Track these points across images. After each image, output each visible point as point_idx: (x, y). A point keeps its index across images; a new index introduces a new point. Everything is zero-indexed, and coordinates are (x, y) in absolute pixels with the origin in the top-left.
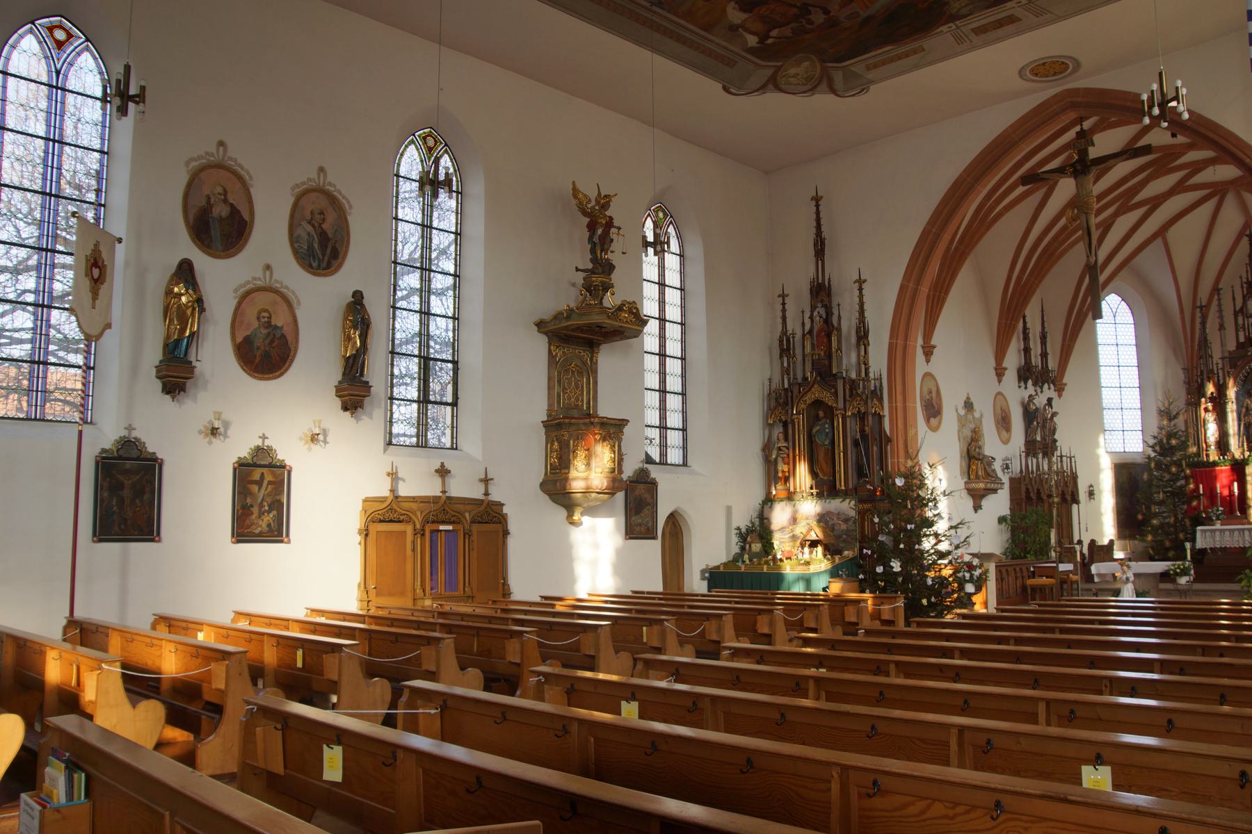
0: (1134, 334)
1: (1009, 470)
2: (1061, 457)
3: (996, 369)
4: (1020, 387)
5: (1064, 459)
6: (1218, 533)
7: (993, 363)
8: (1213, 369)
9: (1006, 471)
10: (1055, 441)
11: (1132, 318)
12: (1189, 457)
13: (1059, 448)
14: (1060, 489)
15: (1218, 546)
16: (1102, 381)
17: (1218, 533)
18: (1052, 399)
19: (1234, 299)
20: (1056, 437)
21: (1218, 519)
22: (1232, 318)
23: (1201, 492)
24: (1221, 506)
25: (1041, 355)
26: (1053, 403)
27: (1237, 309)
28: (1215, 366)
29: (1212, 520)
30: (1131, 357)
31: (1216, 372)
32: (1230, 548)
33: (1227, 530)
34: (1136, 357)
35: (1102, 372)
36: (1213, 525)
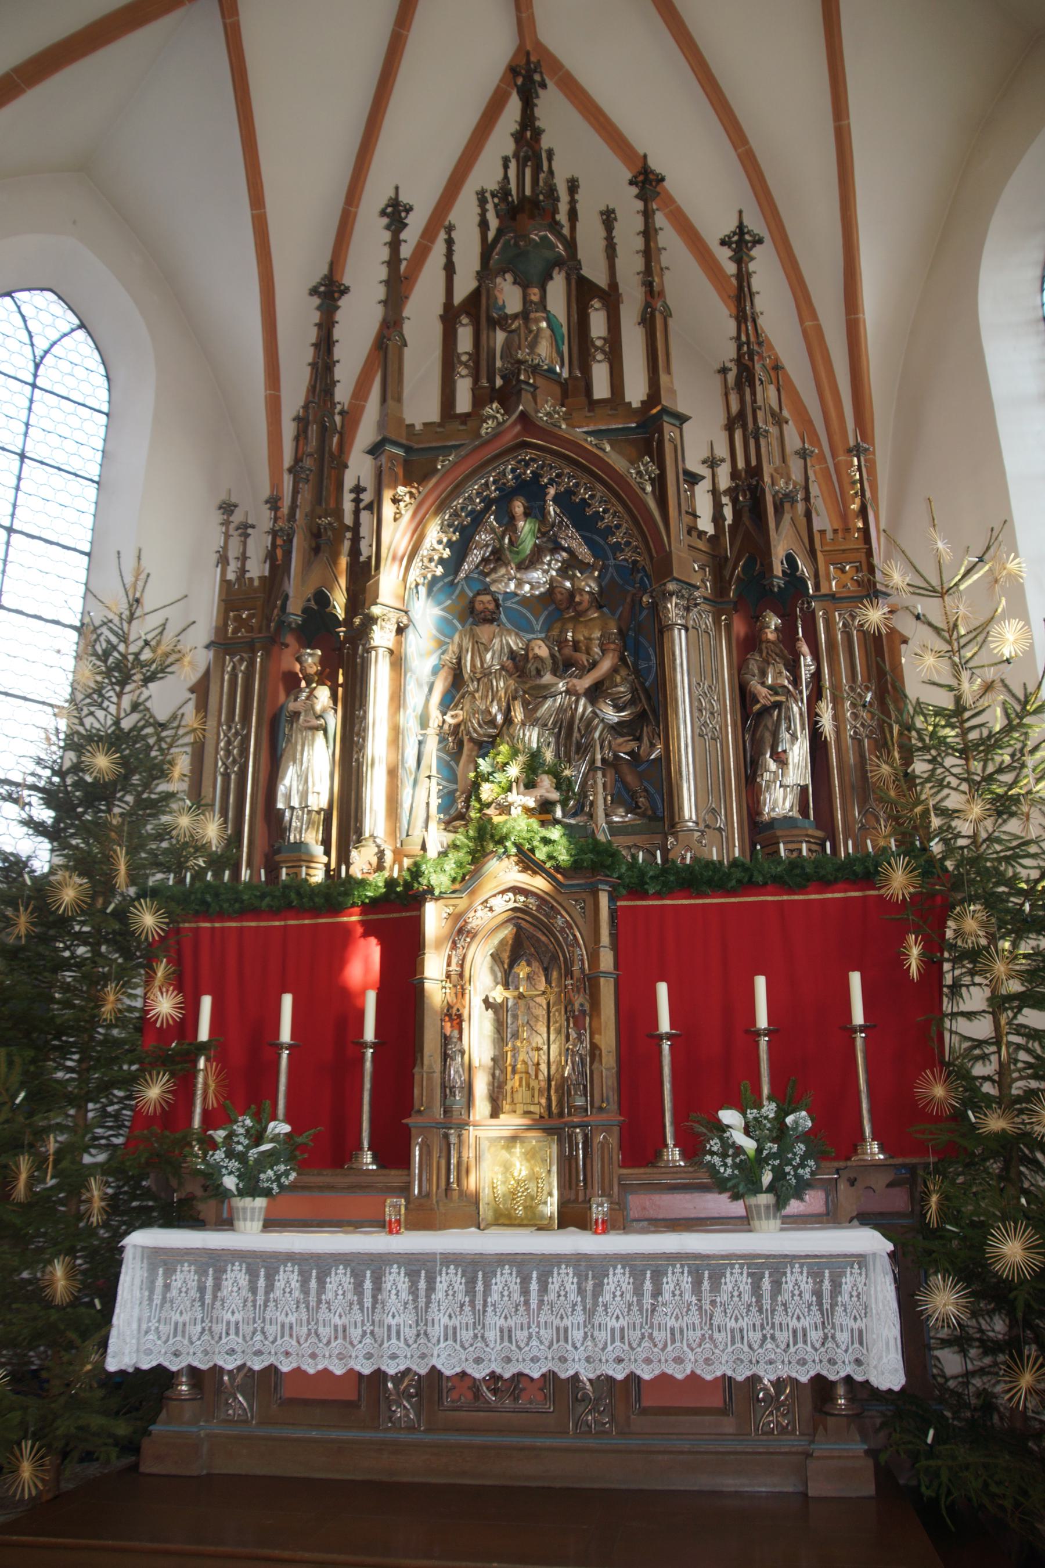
0: (100, 445)
6: (236, 1277)
8: (339, 513)
11: (104, 395)
12: (175, 860)
15: (230, 1364)
17: (236, 1277)
19: (450, 268)
21: (251, 1188)
22: (437, 329)
23: (204, 1034)
24: (288, 1120)
27: (458, 298)
28: (348, 498)
29: (223, 1194)
31: (348, 520)
32: (298, 1371)
33: (290, 1257)
34: (89, 521)
36: (227, 1223)
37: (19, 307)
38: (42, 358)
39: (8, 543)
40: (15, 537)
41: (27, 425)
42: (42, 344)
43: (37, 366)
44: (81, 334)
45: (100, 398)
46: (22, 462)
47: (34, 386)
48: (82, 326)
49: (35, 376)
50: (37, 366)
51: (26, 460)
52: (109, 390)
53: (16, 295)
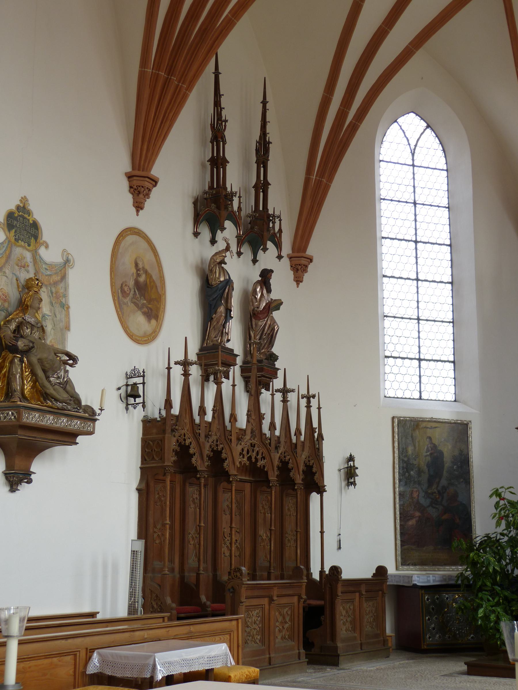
1: (138, 400)
2: (285, 391)
3: (130, 177)
4: (196, 234)
5: (292, 397)
7: (126, 166)
9: (131, 400)
10: (273, 358)
13: (280, 374)
14: (276, 457)
16: (385, 264)
18: (272, 271)
20: (275, 350)
25: (256, 187)
26: (273, 281)
30: (440, 227)
34: (447, 228)
35: (384, 250)
37: (400, 126)
38: (415, 149)
39: (416, 248)
40: (419, 245)
41: (414, 187)
42: (413, 144)
43: (413, 155)
44: (429, 131)
45: (442, 163)
46: (415, 207)
47: (413, 165)
48: (428, 126)
49: (413, 160)
50: (413, 155)
51: (417, 205)
52: (445, 157)
53: (400, 120)
